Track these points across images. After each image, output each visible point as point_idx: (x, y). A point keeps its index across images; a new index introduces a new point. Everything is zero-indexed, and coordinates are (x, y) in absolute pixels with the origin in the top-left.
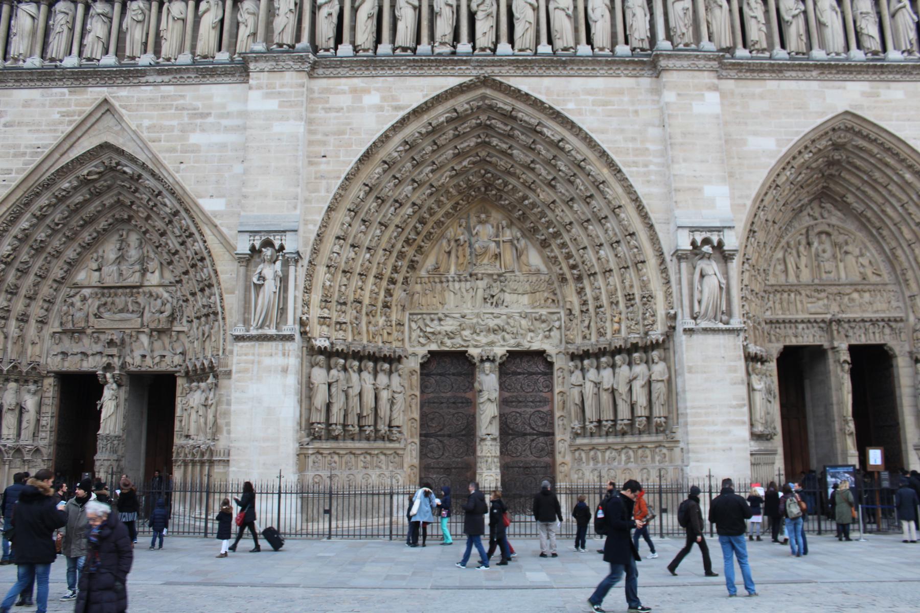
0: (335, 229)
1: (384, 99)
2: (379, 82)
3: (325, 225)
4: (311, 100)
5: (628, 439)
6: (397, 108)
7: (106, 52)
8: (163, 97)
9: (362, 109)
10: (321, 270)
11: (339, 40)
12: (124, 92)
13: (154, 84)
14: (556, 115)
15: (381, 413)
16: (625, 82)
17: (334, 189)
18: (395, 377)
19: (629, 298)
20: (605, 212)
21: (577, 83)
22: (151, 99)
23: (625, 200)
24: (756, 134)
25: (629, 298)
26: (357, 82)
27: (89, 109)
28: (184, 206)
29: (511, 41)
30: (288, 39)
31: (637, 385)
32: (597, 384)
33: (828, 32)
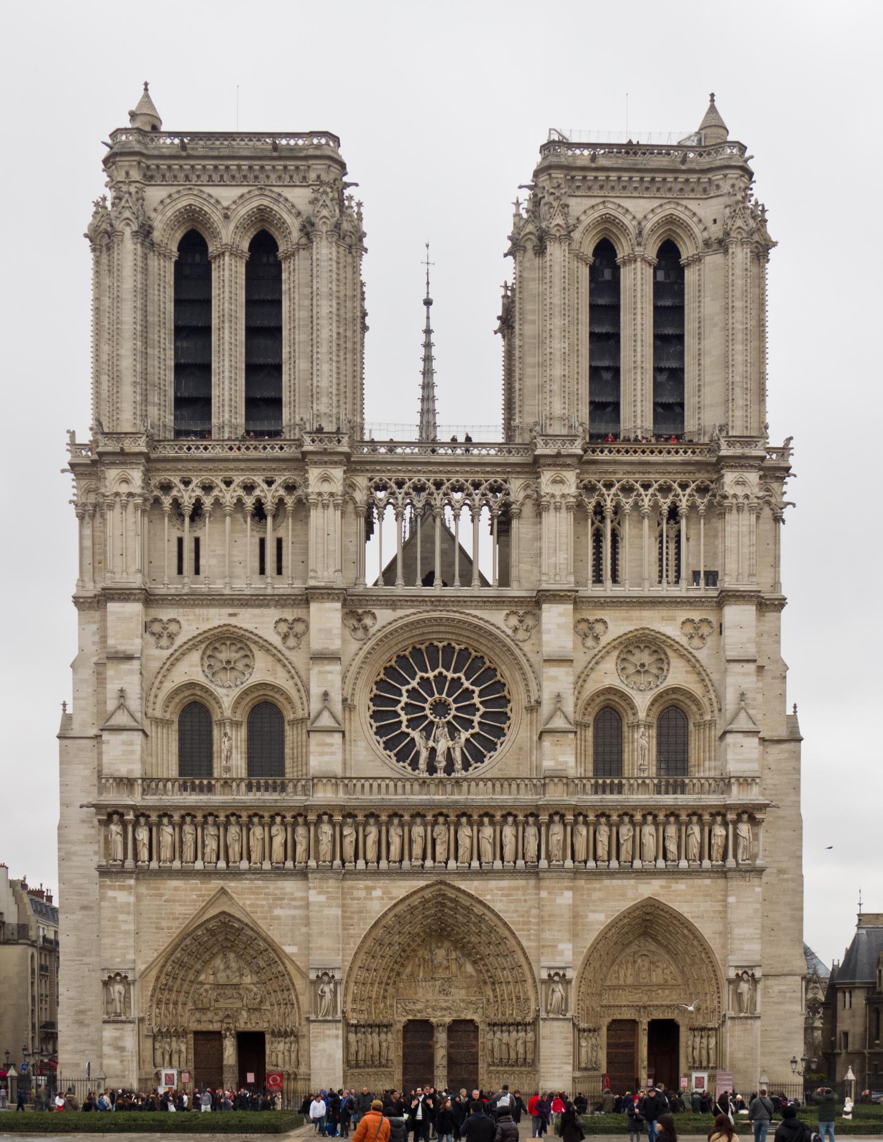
0: (359, 963)
1: (384, 893)
2: (381, 883)
3: (353, 962)
4: (343, 893)
5: (515, 1069)
6: (391, 899)
7: (218, 858)
8: (257, 888)
9: (372, 899)
10: (352, 984)
11: (356, 857)
12: (233, 884)
13: (250, 880)
14: (480, 902)
15: (383, 1054)
16: (521, 883)
17: (358, 943)
18: (389, 1035)
19: (518, 998)
20: (506, 952)
21: (493, 884)
22: (250, 888)
23: (517, 949)
24: (594, 911)
25: (518, 998)
26: (369, 883)
27: (213, 893)
28: (272, 946)
29: (456, 859)
30: (328, 858)
31: (520, 1042)
32: (500, 1040)
33: (646, 849)
